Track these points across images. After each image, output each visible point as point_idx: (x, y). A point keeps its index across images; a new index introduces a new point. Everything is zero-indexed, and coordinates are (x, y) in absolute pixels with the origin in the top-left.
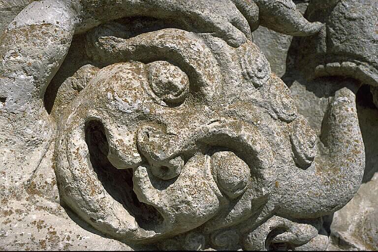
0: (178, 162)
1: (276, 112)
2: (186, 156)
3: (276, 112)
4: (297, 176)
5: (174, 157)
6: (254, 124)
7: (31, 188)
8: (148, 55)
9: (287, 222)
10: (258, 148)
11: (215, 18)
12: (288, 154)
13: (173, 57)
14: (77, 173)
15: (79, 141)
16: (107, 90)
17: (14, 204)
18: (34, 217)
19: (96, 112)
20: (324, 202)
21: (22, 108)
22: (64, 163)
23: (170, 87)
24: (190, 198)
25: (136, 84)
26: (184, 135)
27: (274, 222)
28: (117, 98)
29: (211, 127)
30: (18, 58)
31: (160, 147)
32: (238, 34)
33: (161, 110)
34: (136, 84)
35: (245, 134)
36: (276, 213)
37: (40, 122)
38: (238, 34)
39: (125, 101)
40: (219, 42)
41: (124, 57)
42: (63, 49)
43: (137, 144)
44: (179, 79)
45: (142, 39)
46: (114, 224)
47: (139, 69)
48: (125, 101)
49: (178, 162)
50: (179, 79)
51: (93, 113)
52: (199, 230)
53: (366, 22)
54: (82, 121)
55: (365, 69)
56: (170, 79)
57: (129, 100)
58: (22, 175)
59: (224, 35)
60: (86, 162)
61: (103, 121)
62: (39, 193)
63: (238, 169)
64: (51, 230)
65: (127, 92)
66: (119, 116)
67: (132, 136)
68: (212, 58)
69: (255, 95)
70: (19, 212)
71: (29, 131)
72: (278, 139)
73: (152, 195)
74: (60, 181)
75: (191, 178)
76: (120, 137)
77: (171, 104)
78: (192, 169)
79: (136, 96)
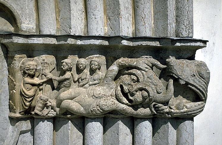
0: (135, 92)
2: (137, 91)
4: (158, 95)
5: (134, 91)
6: (149, 86)
7: (111, 95)
8: (130, 74)
10: (149, 90)
11: (142, 68)
12: (156, 91)
13: (134, 74)
15: (119, 88)
17: (109, 98)
18: (112, 100)
20: (163, 100)
23: (134, 80)
24: (137, 98)
26: (135, 88)
27: (154, 103)
29: (141, 86)
32: (147, 70)
33: (132, 83)
35: (146, 88)
36: (154, 102)
38: (147, 70)
40: (143, 71)
41: (127, 74)
42: (116, 73)
44: (135, 78)
45: (129, 71)
46: (124, 102)
49: (135, 92)
50: (135, 78)
51: (121, 84)
52: (141, 104)
53: (174, 66)
54: (120, 85)
55: (174, 75)
58: (110, 93)
59: (143, 70)
60: (120, 92)
62: (113, 96)
63: (146, 94)
66: (125, 84)
68: (141, 74)
69: (150, 81)
70: (109, 99)
72: (153, 88)
73: (131, 98)
74: (116, 95)
75: (137, 95)
77: (134, 82)
78: (138, 93)
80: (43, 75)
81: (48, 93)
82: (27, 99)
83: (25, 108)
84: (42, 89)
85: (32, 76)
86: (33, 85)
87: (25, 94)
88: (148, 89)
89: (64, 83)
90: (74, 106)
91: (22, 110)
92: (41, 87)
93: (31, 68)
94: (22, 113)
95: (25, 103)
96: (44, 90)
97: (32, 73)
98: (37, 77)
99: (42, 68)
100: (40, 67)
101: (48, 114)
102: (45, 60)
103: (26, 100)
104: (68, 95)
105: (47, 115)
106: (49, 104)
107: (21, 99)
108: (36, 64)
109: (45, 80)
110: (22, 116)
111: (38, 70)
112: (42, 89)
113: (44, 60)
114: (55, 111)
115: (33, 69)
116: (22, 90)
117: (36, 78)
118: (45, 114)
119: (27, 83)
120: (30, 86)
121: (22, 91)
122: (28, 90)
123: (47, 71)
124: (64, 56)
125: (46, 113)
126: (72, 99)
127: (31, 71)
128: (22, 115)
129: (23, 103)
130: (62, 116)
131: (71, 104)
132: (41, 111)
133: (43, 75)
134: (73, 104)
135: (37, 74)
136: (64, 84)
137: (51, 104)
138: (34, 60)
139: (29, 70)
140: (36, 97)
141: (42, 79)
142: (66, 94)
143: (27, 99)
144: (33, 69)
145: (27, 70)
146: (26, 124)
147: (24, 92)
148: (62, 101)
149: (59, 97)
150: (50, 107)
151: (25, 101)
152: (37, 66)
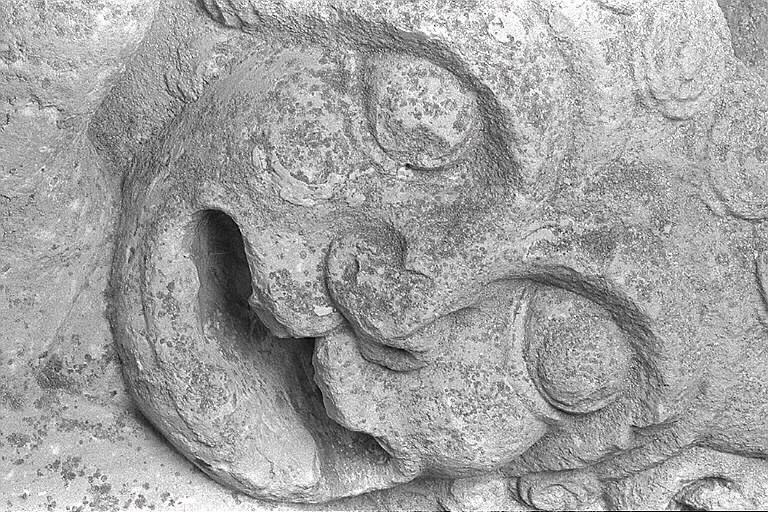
1: (723, 199)
3: (723, 199)
7: (53, 376)
9: (729, 464)
14: (164, 351)
16: (253, 140)
18: (55, 451)
19: (221, 191)
21: (28, 183)
22: (134, 319)
24: (458, 423)
25: (331, 124)
28: (278, 166)
30: (18, 65)
31: (384, 305)
34: (331, 124)
35: (620, 273)
37: (75, 205)
39: (300, 176)
43: (326, 280)
47: (344, 74)
48: (300, 176)
56: (426, 120)
57: (310, 174)
61: (240, 220)
64: (98, 482)
65: (305, 151)
67: (314, 260)
71: (47, 235)
72: (716, 273)
76: (282, 265)
79: (328, 164)
88: (645, 292)
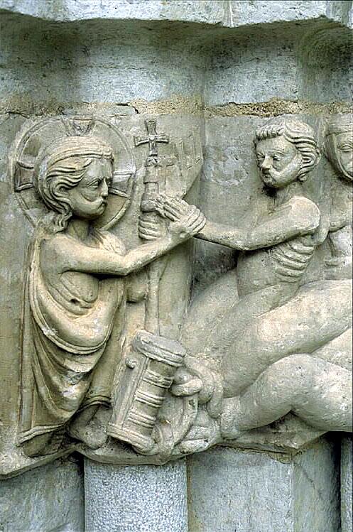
80: (152, 218)
81: (173, 321)
82: (69, 364)
83: (56, 419)
84: (144, 299)
85: (90, 224)
86: (102, 276)
87: (61, 334)
89: (279, 261)
90: (334, 389)
91: (35, 430)
92: (139, 289)
93: (93, 173)
94: (34, 448)
95: (62, 389)
96: (153, 301)
97: (91, 205)
98: (112, 229)
99: (141, 173)
100: (133, 170)
101: (184, 438)
102: (158, 125)
103: (63, 371)
104: (301, 328)
105: (177, 444)
106: (189, 385)
107: (27, 364)
108: (106, 150)
109: (165, 244)
110: (34, 461)
111: (121, 185)
112: (144, 299)
113: (150, 126)
114: (215, 418)
115: (100, 182)
116: (44, 311)
117: (109, 240)
118: (171, 444)
119: (73, 266)
120: (80, 286)
121: (38, 316)
122: (77, 308)
123: (170, 193)
124: (262, 100)
125: (177, 436)
126: (313, 347)
127: (88, 191)
128: (32, 457)
129: (43, 390)
130: (247, 440)
131: (318, 379)
132: (149, 429)
133: (152, 218)
134: (325, 375)
135: (117, 211)
136: (277, 267)
137: (196, 384)
138: (94, 129)
139: (77, 185)
140: (113, 347)
141: (143, 240)
142: (289, 322)
143: (69, 364)
144: (100, 182)
145: (67, 188)
146: (43, 502)
147: (52, 323)
148: (269, 361)
149: (255, 343)
150: (196, 404)
151: (55, 379)
152: (112, 161)
